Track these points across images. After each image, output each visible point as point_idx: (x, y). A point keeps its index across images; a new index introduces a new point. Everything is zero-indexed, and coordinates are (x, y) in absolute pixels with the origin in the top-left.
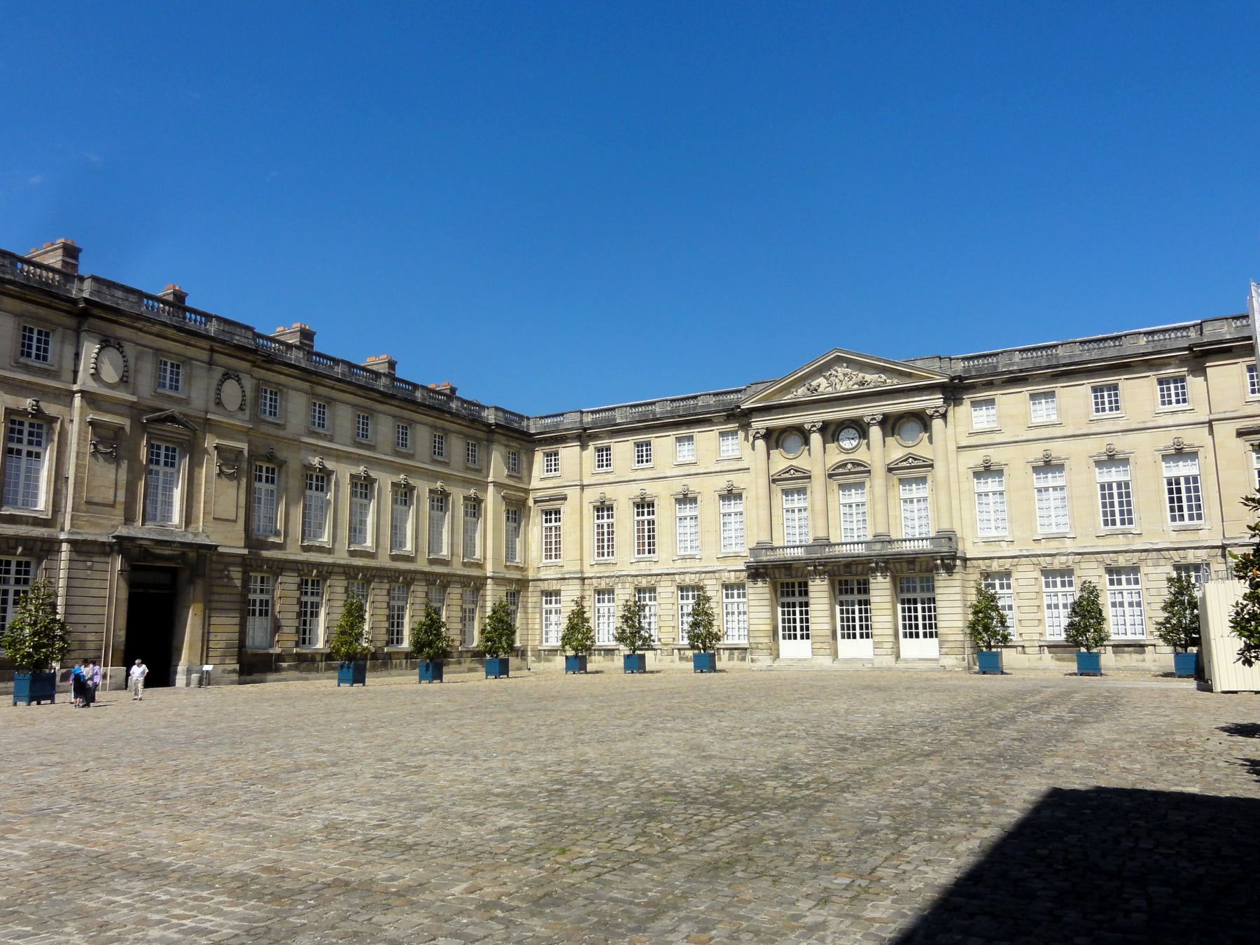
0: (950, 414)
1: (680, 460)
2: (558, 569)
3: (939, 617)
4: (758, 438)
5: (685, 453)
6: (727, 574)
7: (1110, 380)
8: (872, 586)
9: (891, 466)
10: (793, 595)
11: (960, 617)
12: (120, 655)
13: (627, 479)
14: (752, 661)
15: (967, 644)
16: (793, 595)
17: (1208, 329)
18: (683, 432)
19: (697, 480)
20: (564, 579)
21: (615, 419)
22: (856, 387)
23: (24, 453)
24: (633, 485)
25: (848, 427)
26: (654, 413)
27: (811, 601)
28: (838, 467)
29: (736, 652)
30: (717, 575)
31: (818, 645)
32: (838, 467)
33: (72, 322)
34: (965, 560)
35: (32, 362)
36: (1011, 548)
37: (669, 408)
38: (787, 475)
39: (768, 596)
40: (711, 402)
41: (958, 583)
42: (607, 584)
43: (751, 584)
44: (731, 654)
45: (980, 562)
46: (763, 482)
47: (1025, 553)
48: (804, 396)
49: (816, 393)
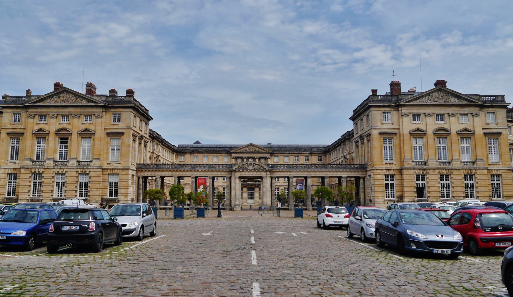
7: (298, 155)
17: (313, 149)
18: (215, 154)
26: (209, 150)
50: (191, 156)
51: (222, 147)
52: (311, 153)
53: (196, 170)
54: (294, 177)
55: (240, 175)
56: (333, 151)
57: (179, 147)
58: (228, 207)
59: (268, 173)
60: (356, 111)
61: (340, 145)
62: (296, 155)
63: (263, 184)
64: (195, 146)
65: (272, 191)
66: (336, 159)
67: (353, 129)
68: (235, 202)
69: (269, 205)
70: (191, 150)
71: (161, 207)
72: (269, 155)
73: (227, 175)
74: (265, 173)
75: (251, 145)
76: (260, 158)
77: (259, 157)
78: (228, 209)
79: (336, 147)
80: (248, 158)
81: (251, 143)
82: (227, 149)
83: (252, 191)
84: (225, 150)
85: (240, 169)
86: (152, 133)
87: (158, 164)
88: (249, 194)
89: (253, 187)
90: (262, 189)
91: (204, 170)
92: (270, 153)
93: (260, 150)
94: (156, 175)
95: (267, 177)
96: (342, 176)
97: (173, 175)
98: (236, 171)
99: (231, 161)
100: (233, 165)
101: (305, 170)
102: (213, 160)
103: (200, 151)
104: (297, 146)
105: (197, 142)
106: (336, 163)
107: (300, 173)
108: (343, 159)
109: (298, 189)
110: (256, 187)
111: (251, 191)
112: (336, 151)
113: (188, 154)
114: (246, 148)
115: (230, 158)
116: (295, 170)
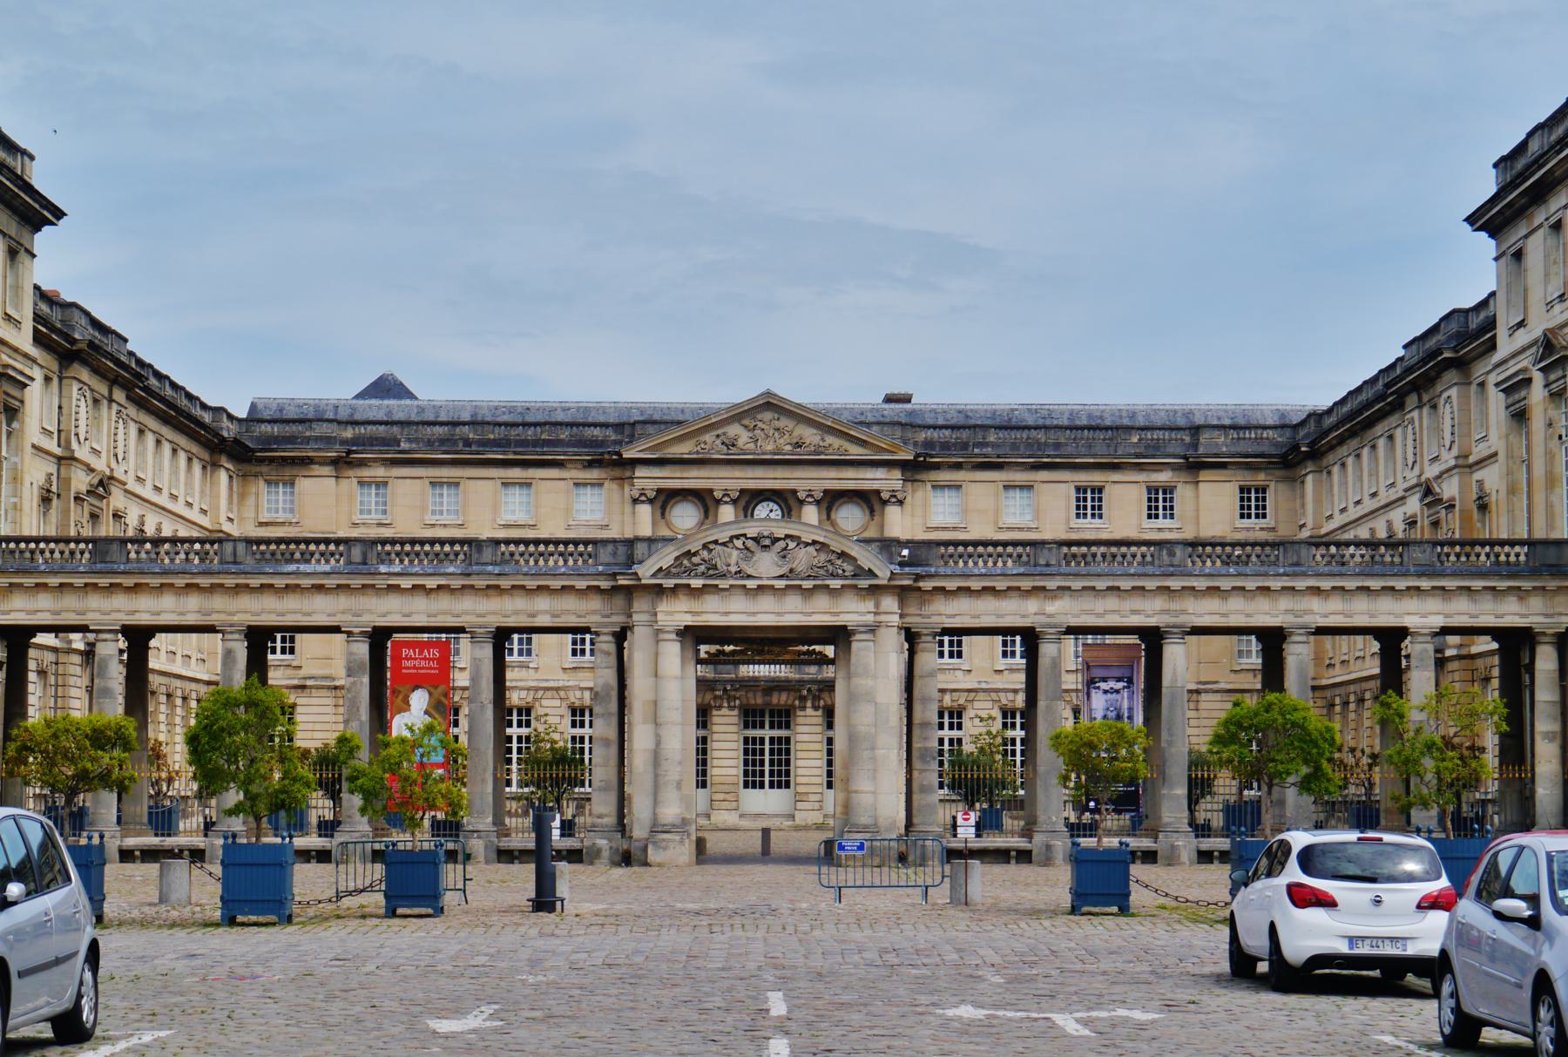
0: (909, 499)
2: (290, 672)
4: (643, 502)
6: (578, 694)
7: (1096, 478)
17: (1205, 437)
18: (516, 473)
20: (303, 687)
22: (789, 448)
26: (468, 443)
30: (562, 693)
31: (721, 796)
36: (968, 677)
37: (492, 436)
40: (562, 437)
47: (984, 686)
50: (344, 483)
51: (560, 417)
52: (1194, 466)
53: (380, 582)
54: (1073, 631)
55: (689, 620)
56: (1343, 451)
57: (254, 418)
58: (602, 843)
59: (890, 603)
60: (1520, 164)
61: (1398, 406)
62: (1084, 478)
63: (849, 677)
64: (371, 416)
65: (916, 732)
66: (1369, 505)
67: (1493, 294)
68: (656, 802)
69: (893, 824)
70: (344, 442)
71: (131, 842)
72: (897, 474)
73: (596, 618)
74: (869, 605)
75: (770, 404)
76: (831, 500)
77: (826, 492)
78: (606, 854)
79: (1370, 423)
80: (749, 500)
81: (768, 393)
82: (597, 432)
83: (776, 733)
85: (689, 572)
86: (56, 316)
87: (109, 540)
88: (751, 749)
89: (780, 699)
90: (848, 717)
91: (431, 583)
92: (903, 465)
93: (830, 439)
94: (90, 619)
95: (882, 631)
96: (1409, 622)
97: (214, 619)
98: (659, 591)
99: (628, 518)
100: (640, 549)
101: (1151, 584)
102: (496, 509)
103: (404, 445)
104: (1090, 416)
105: (385, 387)
106: (1363, 533)
107: (1112, 602)
108: (1414, 505)
109: (1099, 714)
110: (803, 699)
111: (767, 733)
112: (1365, 452)
113: (317, 470)
114: (734, 430)
115: (616, 496)
116: (1077, 584)
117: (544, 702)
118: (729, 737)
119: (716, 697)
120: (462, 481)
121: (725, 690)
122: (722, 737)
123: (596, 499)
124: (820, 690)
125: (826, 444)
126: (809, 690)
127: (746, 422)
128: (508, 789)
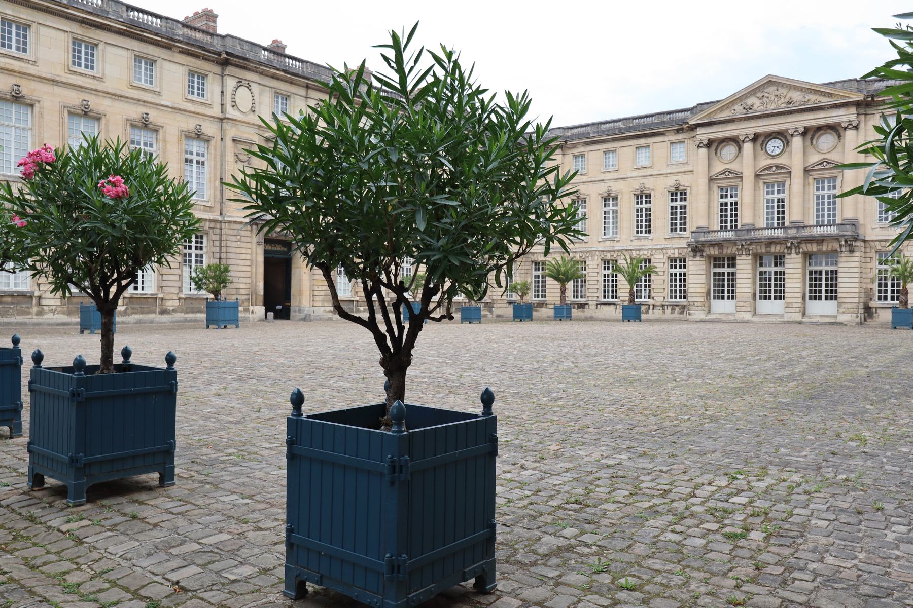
0: (862, 125)
1: (640, 164)
3: (839, 285)
5: (643, 158)
6: (672, 251)
8: (787, 261)
9: (808, 169)
10: (723, 266)
11: (857, 285)
12: (262, 299)
13: (597, 179)
14: (690, 314)
15: (862, 306)
16: (723, 266)
18: (642, 141)
19: (651, 180)
21: (589, 134)
23: (195, 162)
24: (602, 184)
25: (775, 138)
26: (620, 129)
27: (738, 271)
28: (764, 170)
29: (677, 309)
30: (664, 251)
32: (764, 170)
33: (217, 69)
34: (865, 241)
35: (195, 97)
38: (723, 176)
39: (704, 267)
41: (857, 259)
42: (580, 257)
43: (691, 258)
44: (673, 309)
45: (877, 243)
46: (703, 181)
48: (740, 114)
49: (750, 111)
50: (567, 156)
72: (853, 110)
75: (770, 82)
84: (670, 123)
92: (857, 104)
110: (789, 248)
117: (656, 256)
118: (745, 271)
119: (738, 249)
120: (617, 149)
121: (742, 245)
122: (742, 271)
123: (682, 150)
124: (799, 243)
125: (806, 100)
126: (792, 243)
127: (758, 95)
128: (636, 300)
